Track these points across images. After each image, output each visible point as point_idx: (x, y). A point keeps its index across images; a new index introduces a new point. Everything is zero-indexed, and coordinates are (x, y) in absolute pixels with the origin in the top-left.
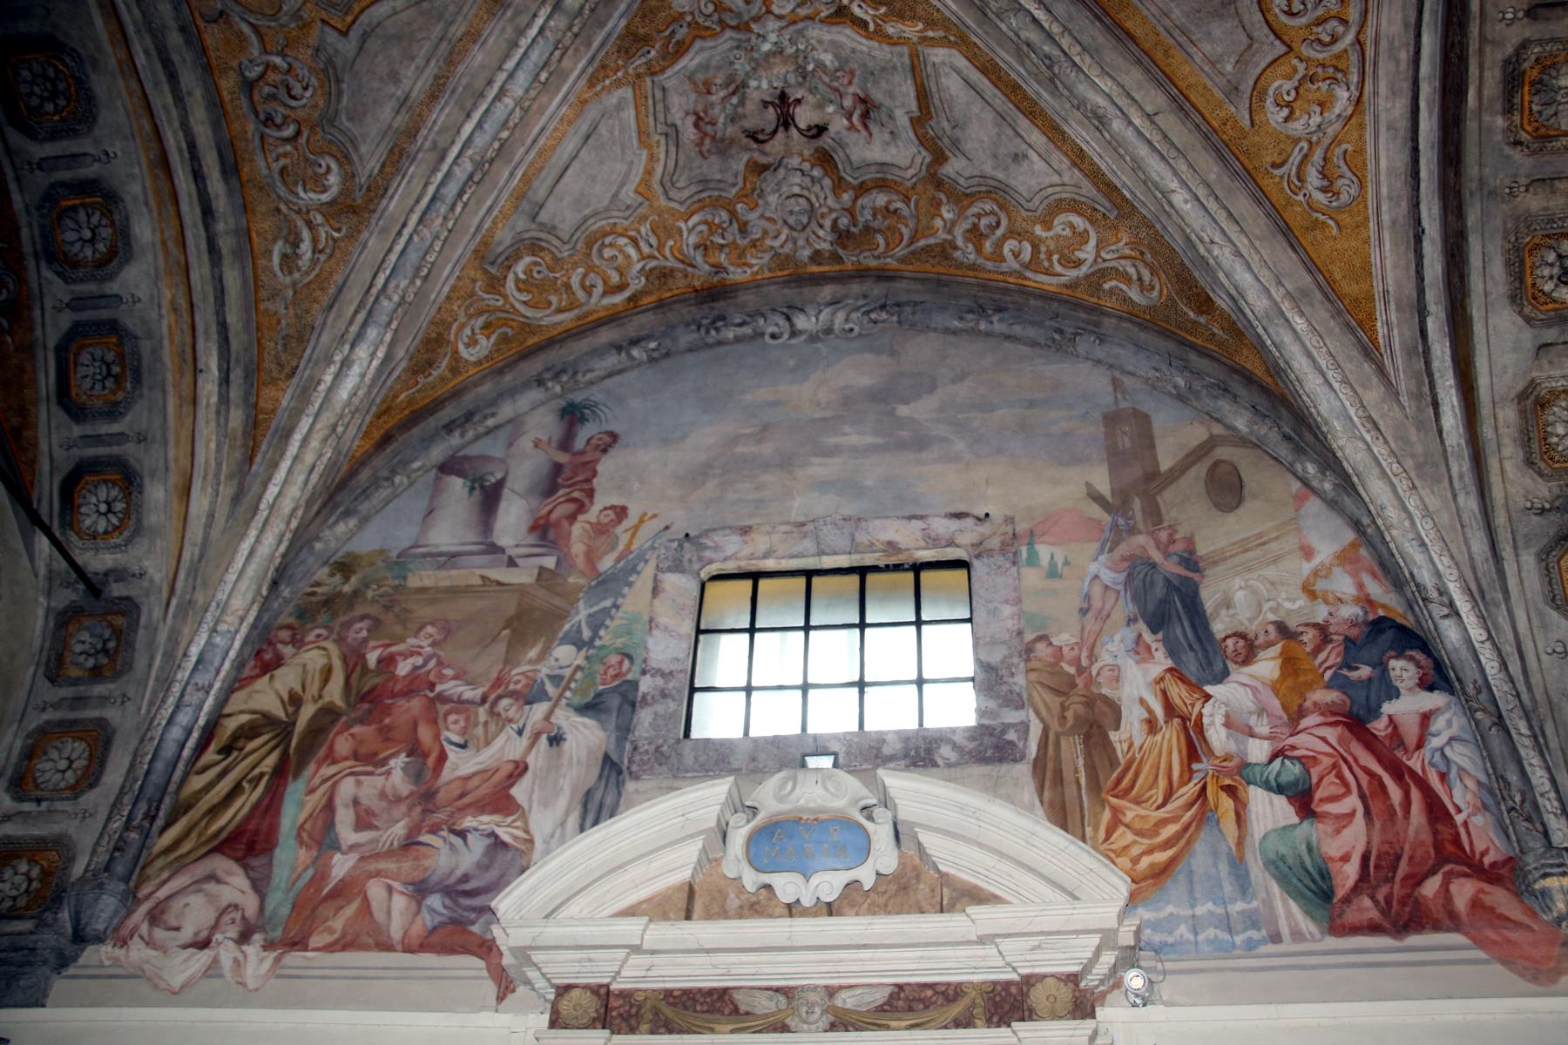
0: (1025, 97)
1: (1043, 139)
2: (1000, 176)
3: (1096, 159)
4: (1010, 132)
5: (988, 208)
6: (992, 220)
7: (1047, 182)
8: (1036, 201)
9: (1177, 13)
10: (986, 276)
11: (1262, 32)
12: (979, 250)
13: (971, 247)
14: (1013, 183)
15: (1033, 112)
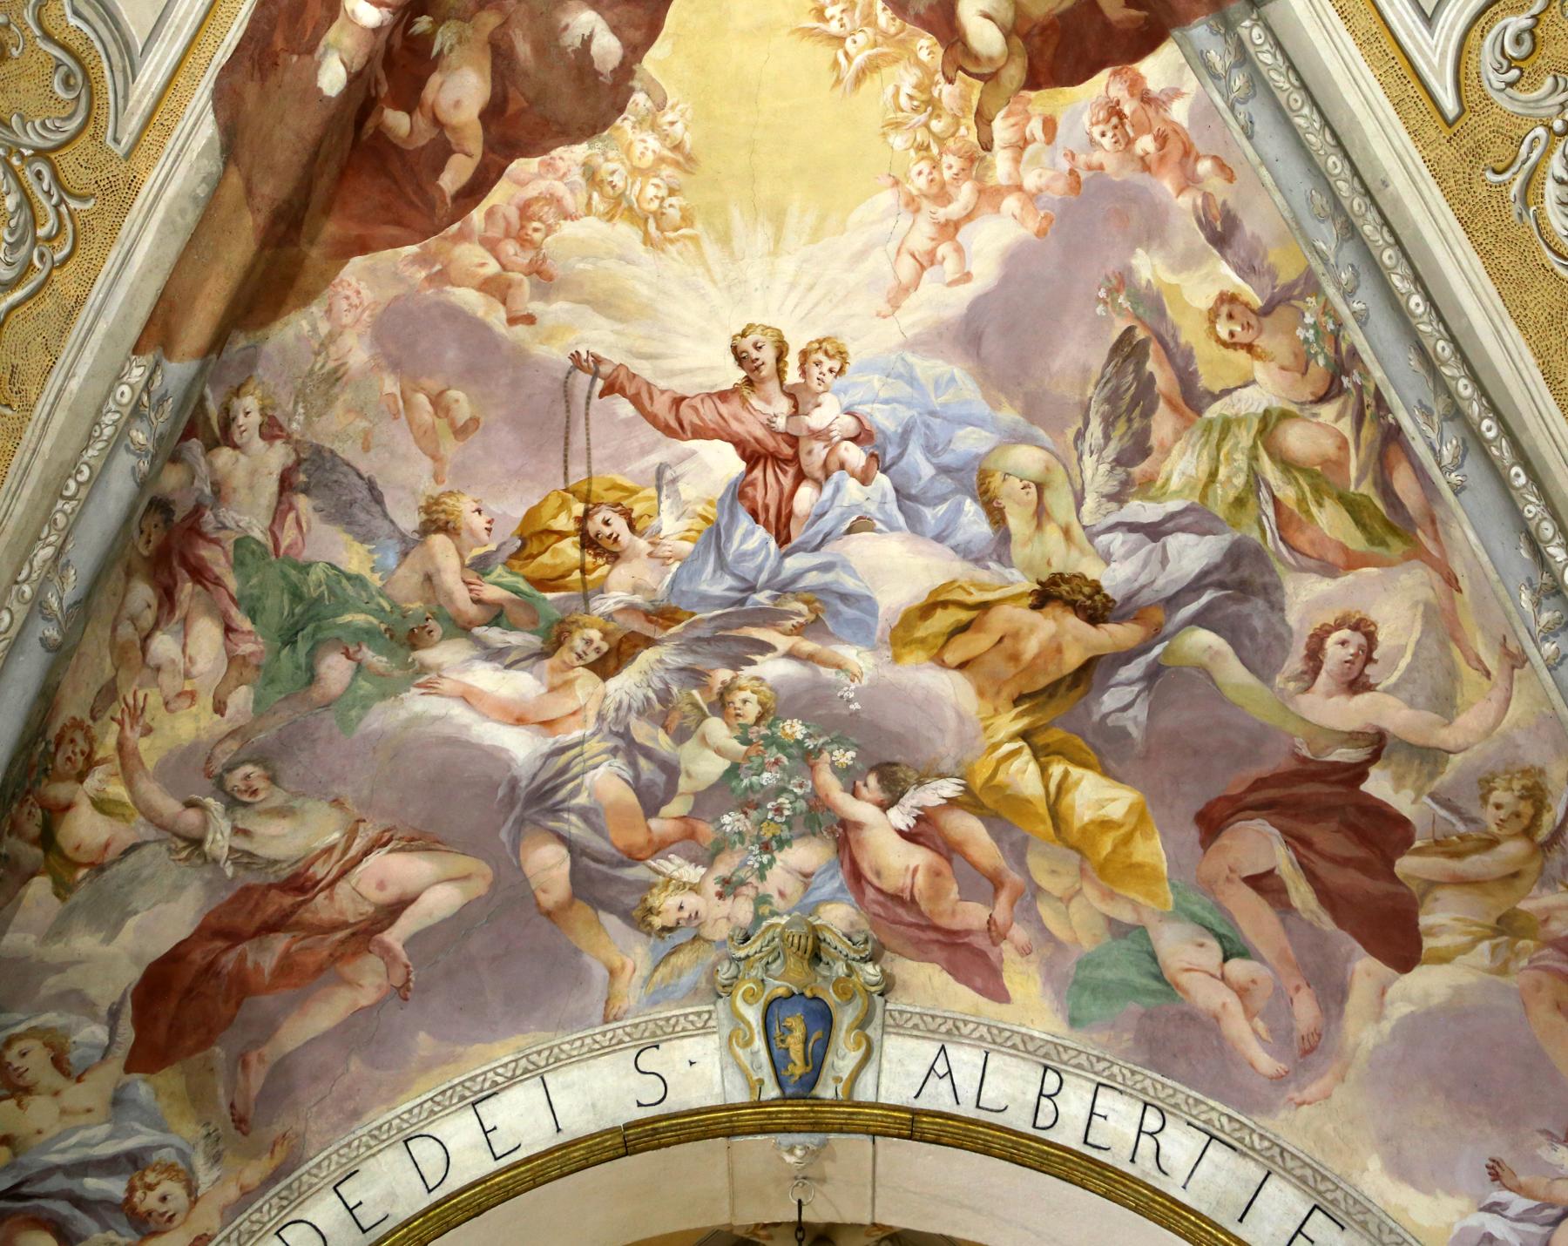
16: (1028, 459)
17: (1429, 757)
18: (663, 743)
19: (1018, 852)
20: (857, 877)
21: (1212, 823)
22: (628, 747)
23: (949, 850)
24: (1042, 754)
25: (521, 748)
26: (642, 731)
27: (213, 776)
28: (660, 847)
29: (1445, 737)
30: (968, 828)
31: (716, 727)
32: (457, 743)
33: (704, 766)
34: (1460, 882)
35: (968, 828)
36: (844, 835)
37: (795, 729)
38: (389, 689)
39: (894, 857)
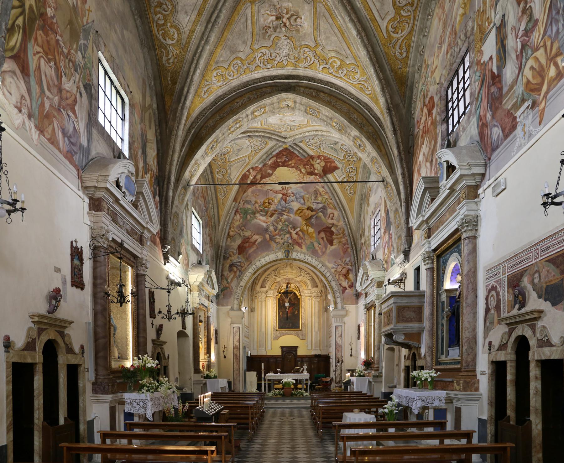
0: (203, 11)
1: (193, 20)
2: (180, 8)
3: (194, 37)
4: (192, 9)
5: (169, 7)
6: (166, 9)
7: (183, 24)
8: (177, 22)
9: (229, 42)
10: (149, 11)
11: (229, 62)
12: (156, 7)
13: (156, 4)
14: (179, 13)
15: (199, 14)
16: (307, 196)
17: (337, 226)
18: (276, 224)
19: (304, 235)
20: (292, 238)
21: (319, 233)
22: (273, 225)
23: (299, 235)
24: (307, 226)
25: (264, 225)
26: (275, 224)
27: (240, 227)
28: (276, 235)
29: (338, 224)
30: (300, 233)
31: (280, 223)
32: (259, 224)
33: (280, 227)
34: (337, 238)
35: (300, 233)
36: (291, 234)
37: (287, 223)
38: (253, 219)
39: (295, 236)
